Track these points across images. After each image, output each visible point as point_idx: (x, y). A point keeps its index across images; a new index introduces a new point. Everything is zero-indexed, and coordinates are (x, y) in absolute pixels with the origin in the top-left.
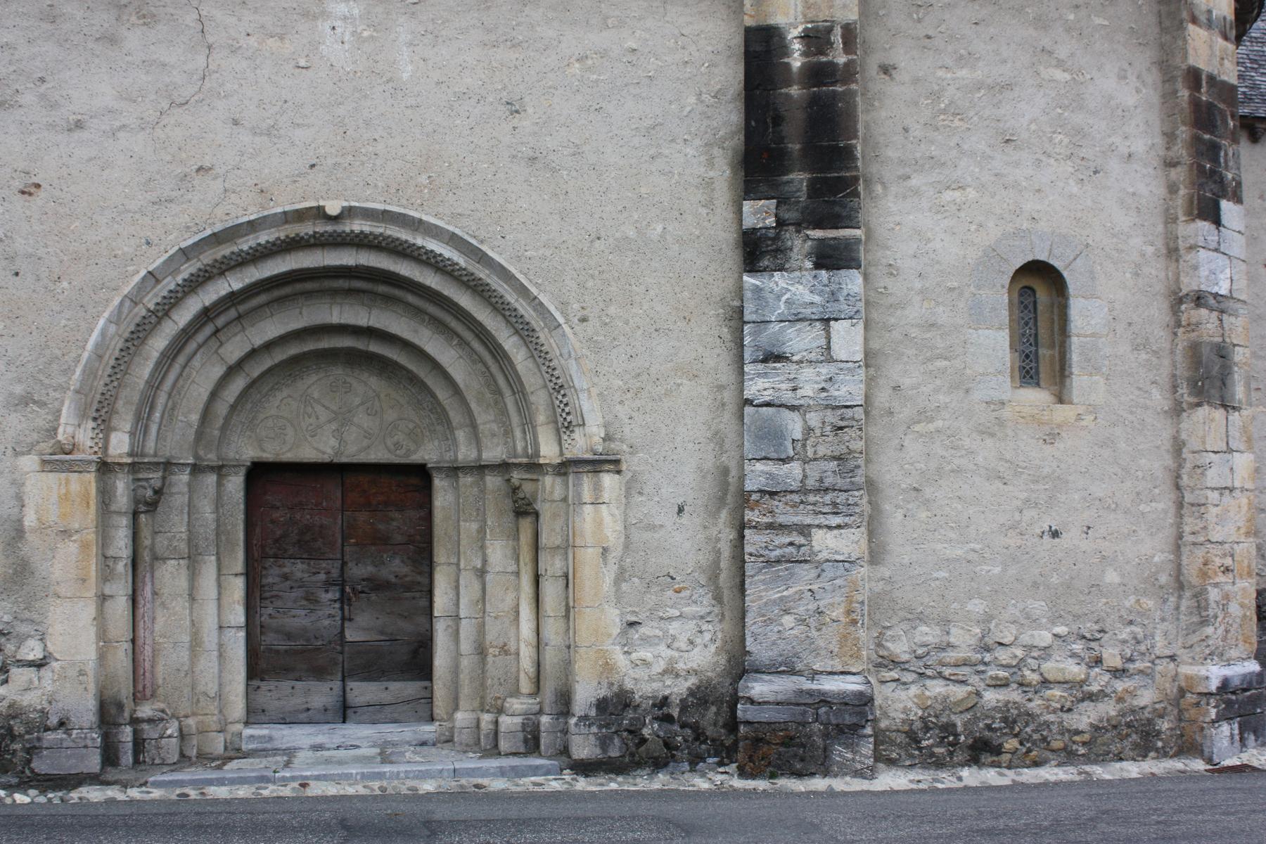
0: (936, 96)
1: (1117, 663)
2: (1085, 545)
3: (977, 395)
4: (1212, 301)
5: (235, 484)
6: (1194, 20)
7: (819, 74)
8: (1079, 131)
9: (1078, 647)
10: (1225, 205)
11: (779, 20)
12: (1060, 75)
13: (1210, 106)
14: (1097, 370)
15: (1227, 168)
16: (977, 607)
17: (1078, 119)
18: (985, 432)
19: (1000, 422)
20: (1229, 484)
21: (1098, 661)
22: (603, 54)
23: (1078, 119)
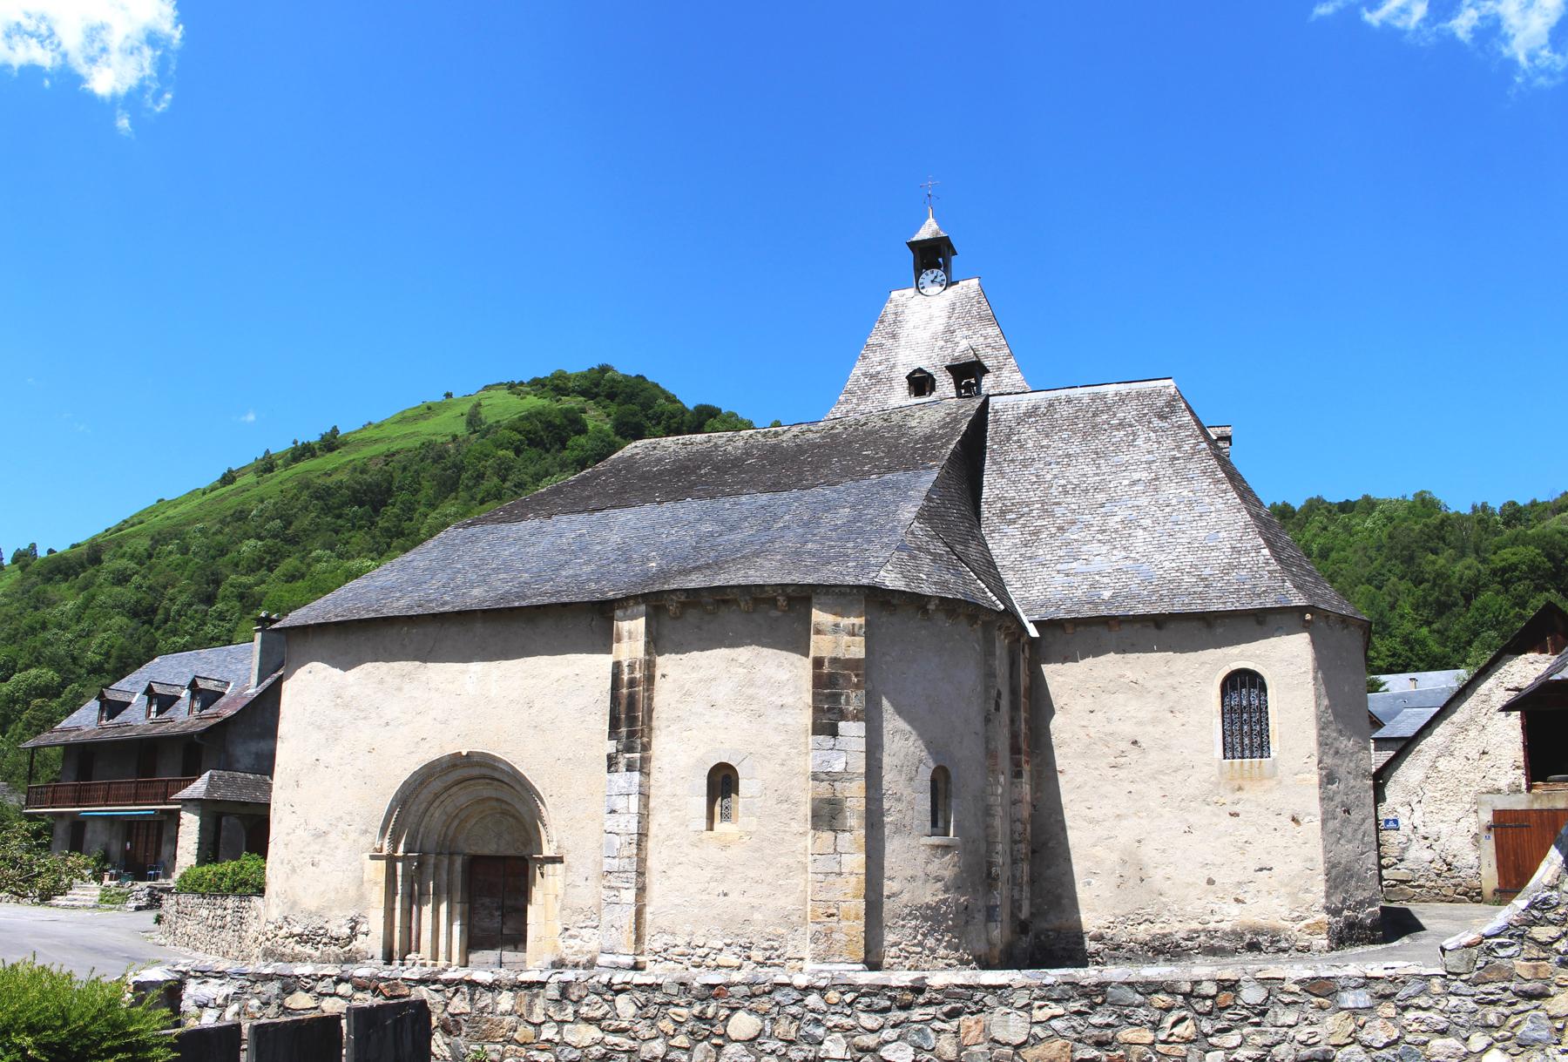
0: (682, 687)
1: (761, 959)
2: (743, 900)
3: (691, 828)
4: (823, 776)
5: (458, 861)
6: (818, 632)
7: (632, 683)
8: (751, 697)
9: (737, 950)
10: (841, 724)
11: (621, 659)
12: (741, 670)
13: (830, 675)
14: (753, 814)
15: (848, 703)
16: (688, 928)
17: (750, 691)
18: (694, 845)
19: (701, 840)
20: (837, 870)
21: (749, 958)
22: (566, 677)
23: (750, 691)
